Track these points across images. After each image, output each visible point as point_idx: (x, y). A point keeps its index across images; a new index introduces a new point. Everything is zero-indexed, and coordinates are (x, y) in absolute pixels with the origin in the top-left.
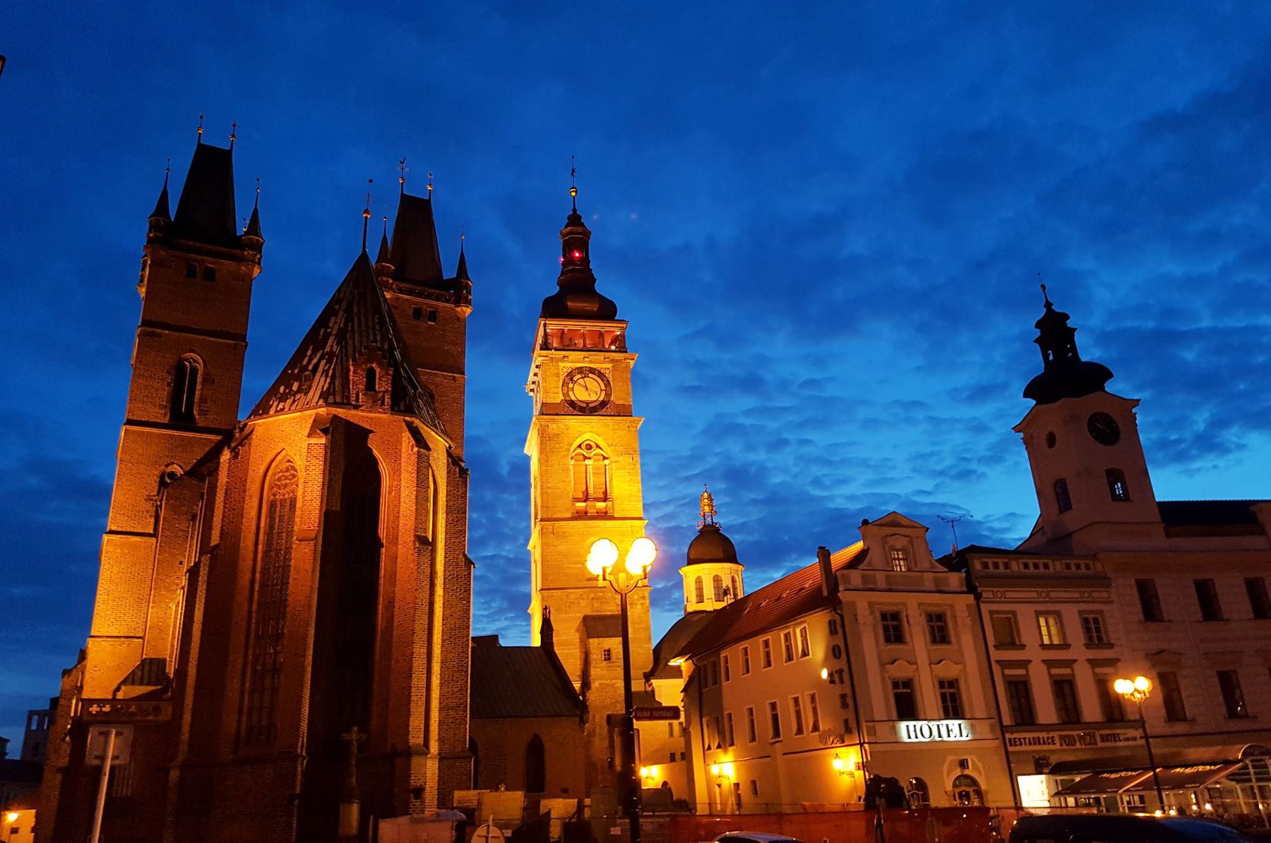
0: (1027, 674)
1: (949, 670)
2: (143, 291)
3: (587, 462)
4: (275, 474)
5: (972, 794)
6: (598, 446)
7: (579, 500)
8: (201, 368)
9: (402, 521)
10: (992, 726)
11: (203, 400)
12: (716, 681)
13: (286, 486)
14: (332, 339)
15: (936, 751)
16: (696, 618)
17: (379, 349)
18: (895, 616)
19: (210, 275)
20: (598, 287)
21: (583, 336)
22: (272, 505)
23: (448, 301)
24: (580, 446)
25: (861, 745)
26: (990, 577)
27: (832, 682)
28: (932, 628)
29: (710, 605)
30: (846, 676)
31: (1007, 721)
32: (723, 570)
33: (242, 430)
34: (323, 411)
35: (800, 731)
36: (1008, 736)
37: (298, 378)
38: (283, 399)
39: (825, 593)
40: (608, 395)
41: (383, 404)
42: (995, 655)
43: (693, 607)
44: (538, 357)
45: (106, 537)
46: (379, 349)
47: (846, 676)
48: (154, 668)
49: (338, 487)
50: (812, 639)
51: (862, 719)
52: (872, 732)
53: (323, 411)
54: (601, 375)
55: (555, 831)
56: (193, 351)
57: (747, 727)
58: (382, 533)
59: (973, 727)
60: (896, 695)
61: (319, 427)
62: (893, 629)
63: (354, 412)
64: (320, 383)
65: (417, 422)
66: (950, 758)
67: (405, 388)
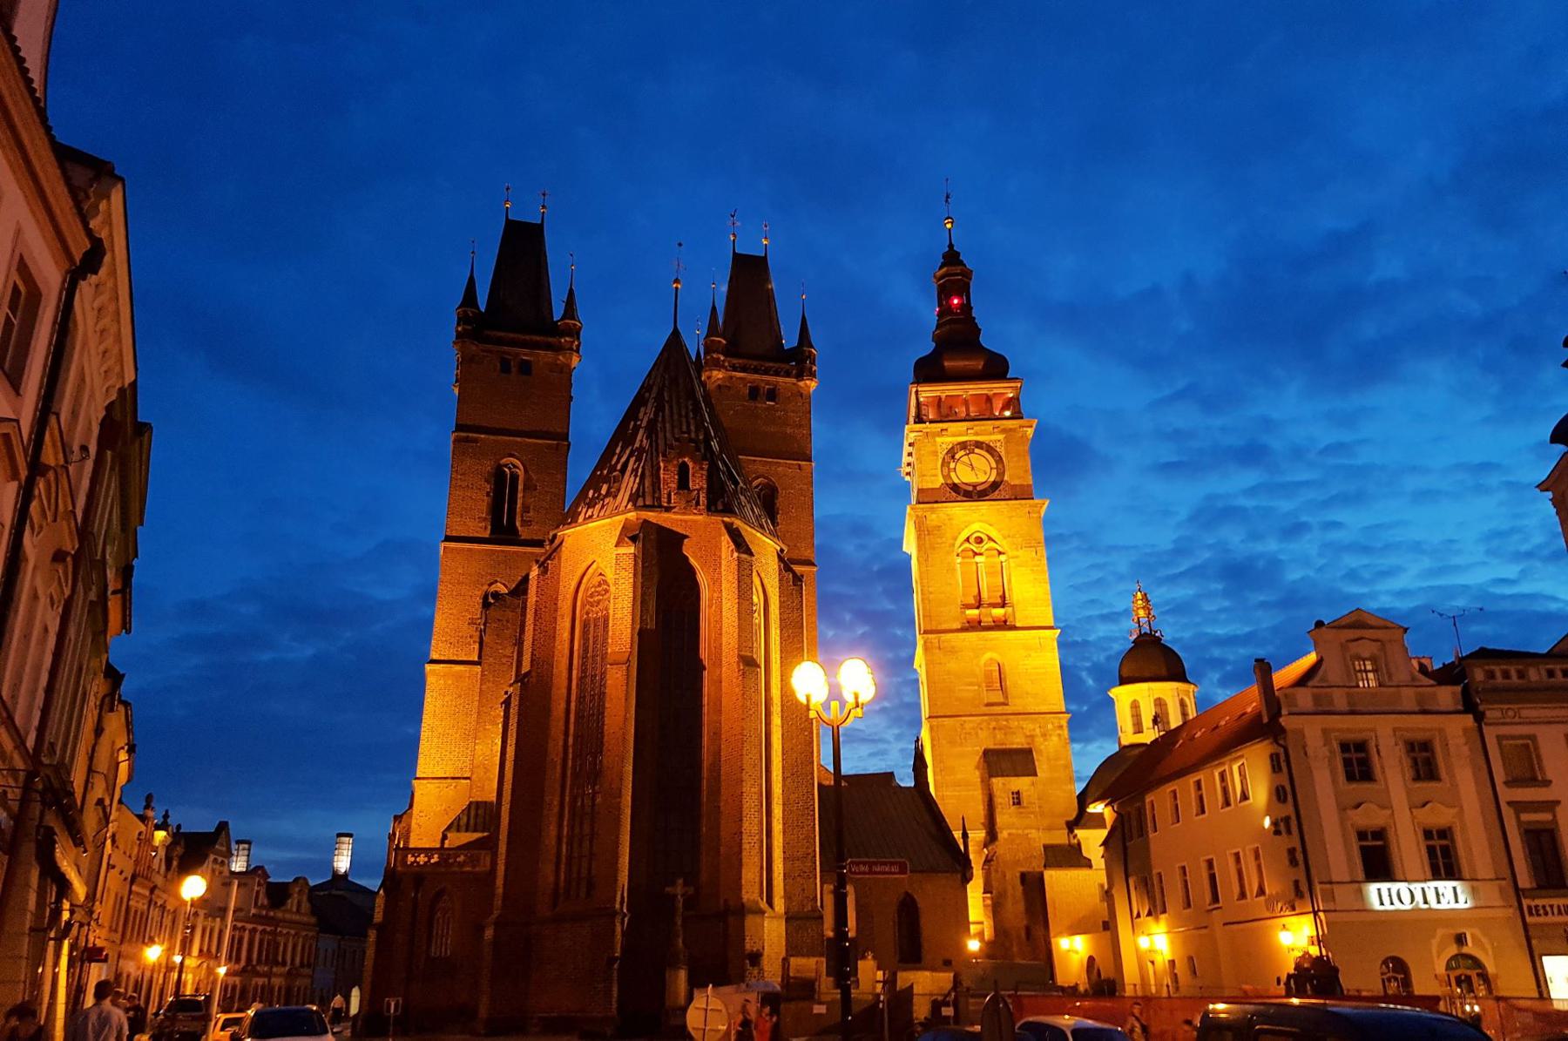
0: (1555, 821)
1: (1439, 816)
2: (456, 391)
3: (978, 559)
4: (587, 590)
5: (1475, 979)
6: (990, 539)
8: (521, 473)
9: (724, 640)
10: (1501, 889)
11: (526, 509)
12: (1142, 832)
13: (598, 602)
14: (641, 432)
15: (1422, 922)
16: (1136, 752)
17: (691, 440)
18: (1361, 746)
19: (526, 368)
20: (985, 341)
21: (966, 403)
22: (586, 625)
23: (788, 375)
24: (967, 540)
25: (1315, 913)
26: (1495, 690)
27: (1277, 832)
28: (1415, 760)
29: (1149, 735)
30: (1294, 823)
31: (1525, 881)
32: (1167, 690)
33: (552, 541)
34: (632, 515)
35: (1243, 895)
36: (1525, 902)
37: (606, 480)
38: (591, 505)
39: (1265, 720)
40: (1001, 473)
41: (698, 503)
43: (1129, 738)
44: (911, 432)
45: (428, 667)
46: (691, 440)
47: (1294, 823)
48: (480, 812)
49: (652, 604)
50: (1251, 777)
51: (1316, 881)
52: (1330, 897)
53: (632, 515)
54: (990, 450)
55: (921, 1010)
56: (511, 455)
57: (1180, 885)
58: (704, 654)
59: (1474, 892)
60: (1362, 848)
61: (629, 535)
62: (1358, 763)
63: (666, 515)
64: (629, 483)
65: (738, 523)
66: (1440, 932)
67: (723, 484)
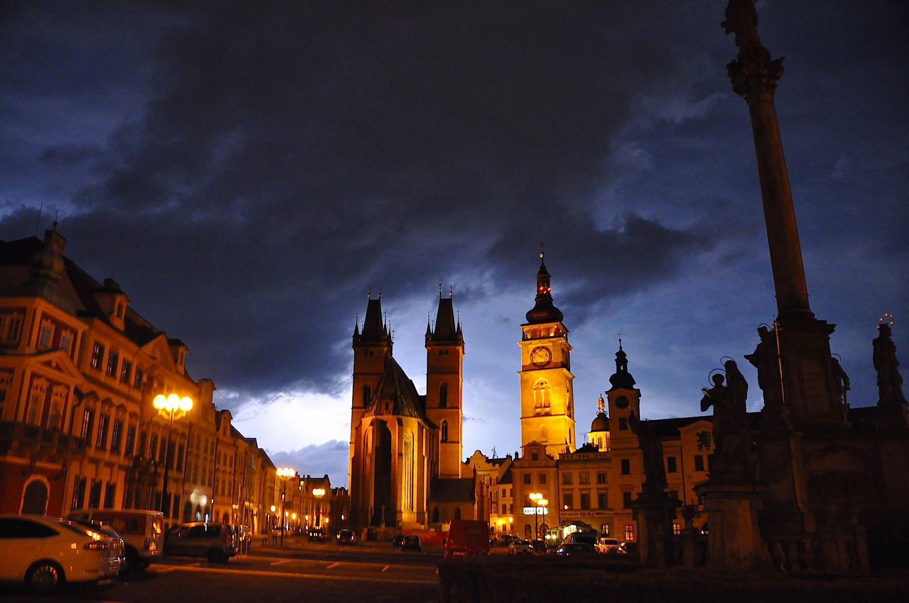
7: (537, 408)
19: (372, 353)
42: (561, 487)
64: (375, 407)
